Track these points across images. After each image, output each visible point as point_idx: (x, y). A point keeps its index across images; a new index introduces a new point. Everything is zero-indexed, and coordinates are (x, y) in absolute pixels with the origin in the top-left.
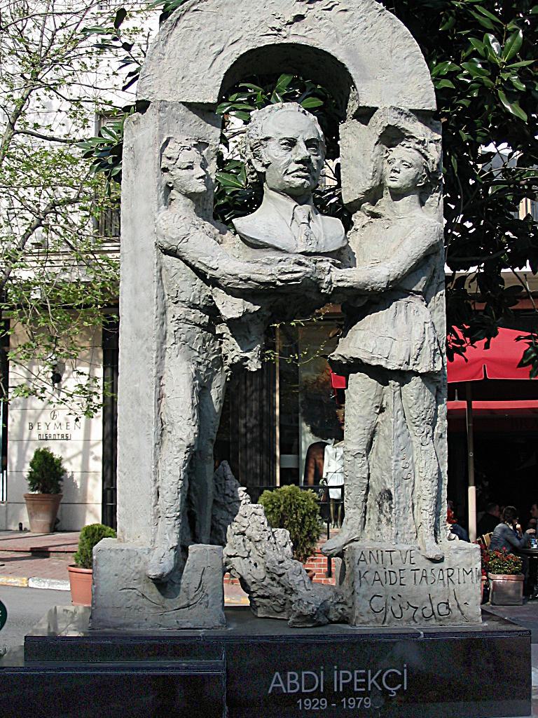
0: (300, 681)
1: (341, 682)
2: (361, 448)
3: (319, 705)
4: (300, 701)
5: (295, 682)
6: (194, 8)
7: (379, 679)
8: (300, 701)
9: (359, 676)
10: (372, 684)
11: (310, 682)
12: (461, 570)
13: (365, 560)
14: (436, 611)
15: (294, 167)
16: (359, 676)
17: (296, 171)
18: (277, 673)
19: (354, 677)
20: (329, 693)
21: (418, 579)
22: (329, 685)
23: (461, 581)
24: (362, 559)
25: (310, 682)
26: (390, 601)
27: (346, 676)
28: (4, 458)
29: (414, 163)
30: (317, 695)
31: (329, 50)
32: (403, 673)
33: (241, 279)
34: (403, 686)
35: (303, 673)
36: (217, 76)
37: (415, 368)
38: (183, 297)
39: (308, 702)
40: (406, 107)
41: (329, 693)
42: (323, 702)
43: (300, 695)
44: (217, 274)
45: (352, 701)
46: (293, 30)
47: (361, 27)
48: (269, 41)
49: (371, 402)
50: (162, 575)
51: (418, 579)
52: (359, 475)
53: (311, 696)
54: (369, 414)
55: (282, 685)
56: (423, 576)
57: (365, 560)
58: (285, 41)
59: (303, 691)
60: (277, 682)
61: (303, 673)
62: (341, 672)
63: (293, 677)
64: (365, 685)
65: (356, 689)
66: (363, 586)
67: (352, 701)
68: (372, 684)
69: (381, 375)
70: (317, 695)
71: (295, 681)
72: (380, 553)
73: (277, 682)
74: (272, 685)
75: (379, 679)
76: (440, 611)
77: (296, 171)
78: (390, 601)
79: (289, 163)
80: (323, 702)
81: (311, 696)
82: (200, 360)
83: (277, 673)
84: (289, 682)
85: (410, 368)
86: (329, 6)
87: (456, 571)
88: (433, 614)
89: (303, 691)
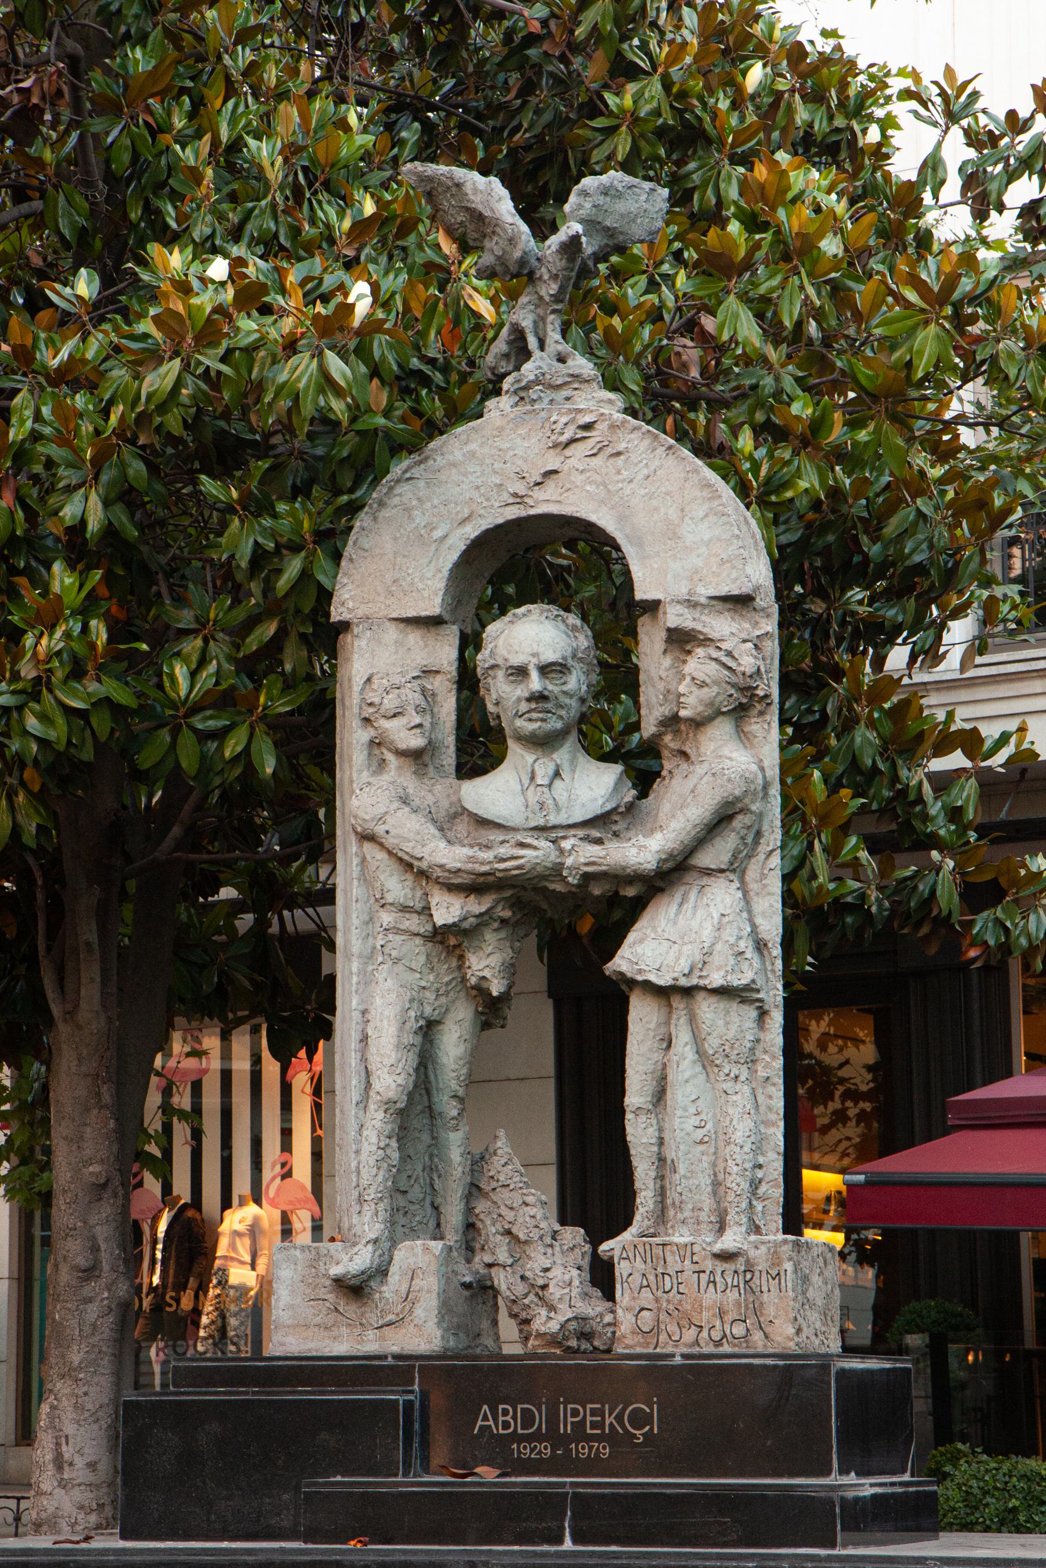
0: (515, 1418)
1: (570, 1419)
2: (642, 1100)
3: (540, 1453)
4: (515, 1446)
5: (508, 1418)
6: (408, 475)
7: (619, 1418)
8: (515, 1446)
9: (593, 1412)
10: (611, 1424)
11: (528, 1419)
12: (764, 1274)
13: (628, 1258)
14: (728, 1332)
15: (524, 707)
16: (593, 1412)
17: (528, 712)
18: (485, 1407)
19: (587, 1412)
20: (553, 1436)
21: (703, 1284)
22: (553, 1420)
23: (765, 1289)
24: (624, 1255)
25: (528, 1419)
26: (663, 1316)
27: (575, 1413)
28: (286, 1126)
29: (708, 681)
30: (537, 1437)
31: (593, 518)
32: (652, 1410)
33: (449, 871)
34: (652, 1429)
35: (519, 1407)
36: (440, 575)
37: (702, 982)
38: (390, 898)
39: (525, 1448)
40: (704, 592)
41: (553, 1436)
42: (546, 1448)
43: (515, 1437)
44: (424, 865)
45: (583, 1448)
46: (538, 494)
47: (640, 476)
48: (513, 513)
49: (652, 1034)
50: (344, 1275)
51: (703, 1284)
52: (644, 1140)
53: (529, 1438)
54: (650, 1050)
55: (491, 1423)
56: (709, 1282)
57: (628, 1258)
58: (532, 512)
59: (520, 1431)
60: (485, 1418)
61: (519, 1407)
62: (570, 1406)
63: (505, 1413)
64: (601, 1425)
65: (589, 1431)
66: (626, 1295)
67: (583, 1448)
68: (611, 1424)
69: (663, 993)
70: (537, 1437)
71: (508, 1418)
72: (648, 1247)
73: (485, 1418)
74: (479, 1423)
75: (619, 1418)
76: (734, 1331)
77: (528, 712)
78: (663, 1316)
79: (519, 700)
80: (546, 1448)
81: (529, 1438)
82: (423, 983)
83: (485, 1407)
84: (501, 1419)
85: (694, 981)
86: (595, 451)
87: (757, 1274)
88: (725, 1336)
89: (520, 1431)
